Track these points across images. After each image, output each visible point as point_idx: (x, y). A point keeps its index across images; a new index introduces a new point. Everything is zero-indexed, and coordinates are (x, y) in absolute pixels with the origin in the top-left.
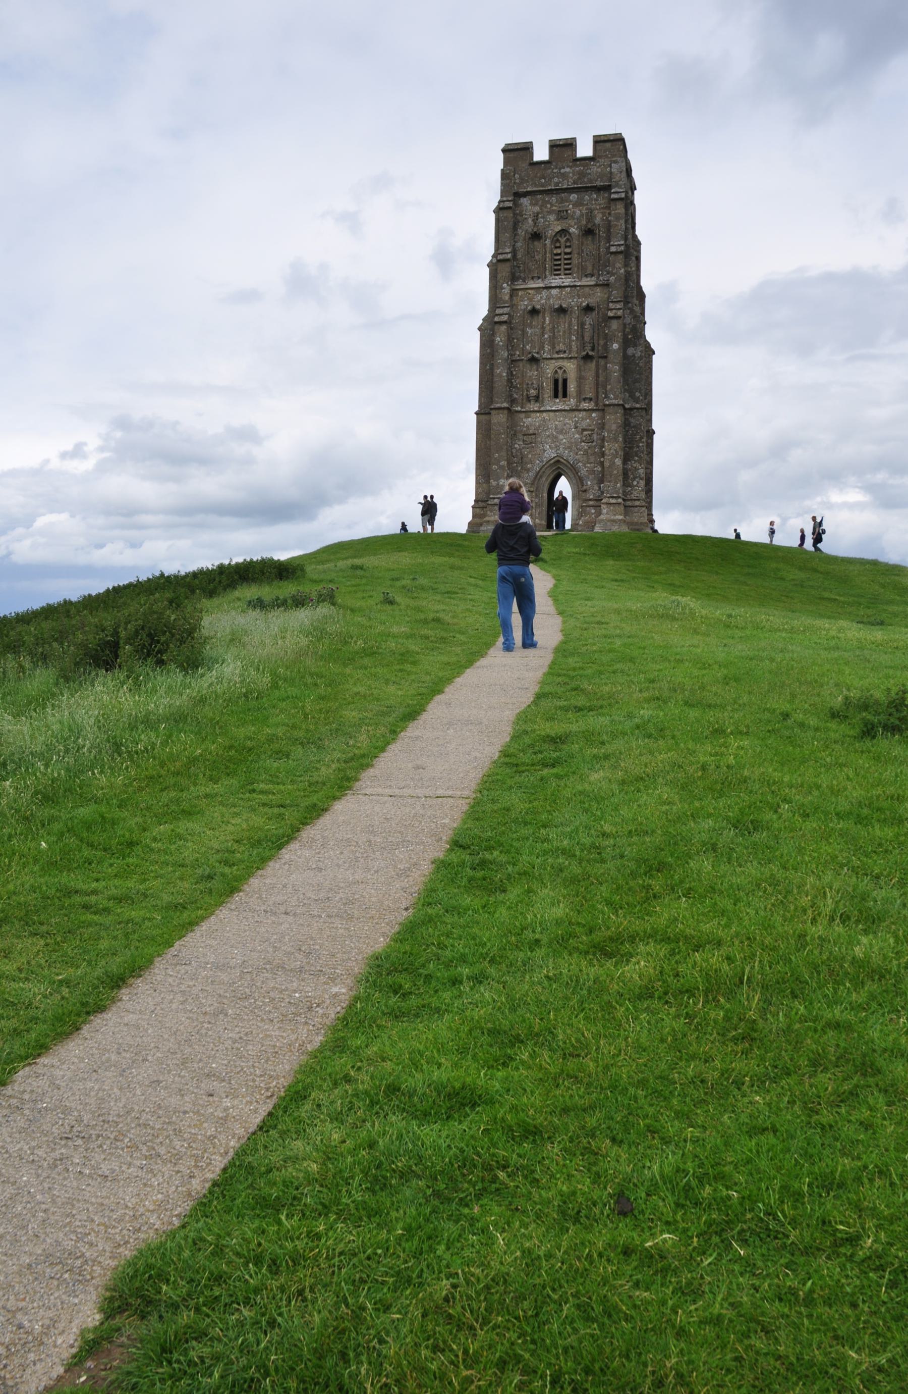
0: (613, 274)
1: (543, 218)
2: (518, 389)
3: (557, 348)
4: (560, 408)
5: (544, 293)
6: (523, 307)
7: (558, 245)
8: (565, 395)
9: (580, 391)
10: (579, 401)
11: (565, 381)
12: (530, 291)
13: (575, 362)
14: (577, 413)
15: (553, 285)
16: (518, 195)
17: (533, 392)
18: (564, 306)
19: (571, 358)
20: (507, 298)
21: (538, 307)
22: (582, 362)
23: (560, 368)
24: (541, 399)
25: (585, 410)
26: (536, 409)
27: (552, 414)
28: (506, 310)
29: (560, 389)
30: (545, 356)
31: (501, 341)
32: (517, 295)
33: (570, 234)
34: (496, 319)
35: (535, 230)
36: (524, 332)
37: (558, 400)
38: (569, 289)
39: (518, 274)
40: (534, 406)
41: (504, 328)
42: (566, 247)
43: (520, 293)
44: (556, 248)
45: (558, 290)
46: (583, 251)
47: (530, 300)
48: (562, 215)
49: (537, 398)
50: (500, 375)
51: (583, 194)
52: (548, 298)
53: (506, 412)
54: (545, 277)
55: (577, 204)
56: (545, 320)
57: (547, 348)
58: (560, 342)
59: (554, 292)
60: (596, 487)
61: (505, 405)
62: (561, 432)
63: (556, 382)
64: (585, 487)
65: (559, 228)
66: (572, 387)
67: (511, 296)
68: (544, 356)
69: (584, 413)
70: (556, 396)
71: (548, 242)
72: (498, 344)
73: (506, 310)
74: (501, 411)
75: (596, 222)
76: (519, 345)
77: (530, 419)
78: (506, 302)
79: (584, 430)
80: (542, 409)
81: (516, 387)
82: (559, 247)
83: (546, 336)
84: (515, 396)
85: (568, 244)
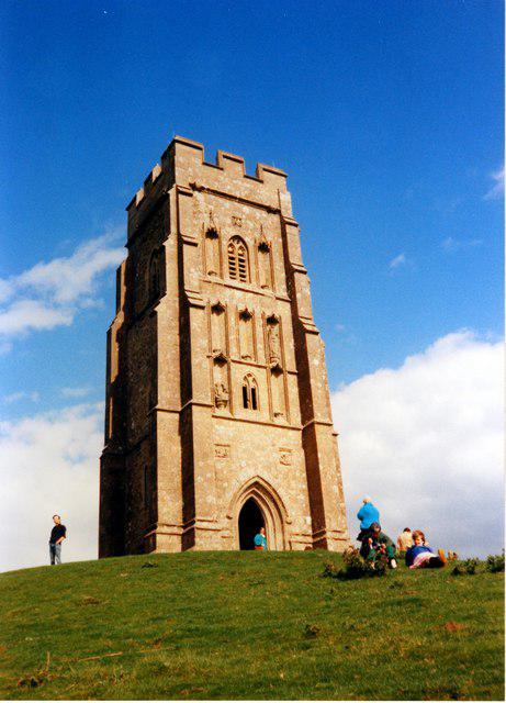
7: (230, 249)
9: (270, 405)
11: (253, 390)
16: (193, 186)
17: (225, 397)
19: (260, 367)
21: (223, 303)
23: (249, 375)
33: (244, 242)
48: (236, 222)
51: (255, 210)
55: (251, 218)
60: (301, 521)
62: (258, 448)
63: (244, 389)
64: (289, 519)
66: (262, 397)
71: (225, 243)
77: (222, 427)
79: (282, 450)
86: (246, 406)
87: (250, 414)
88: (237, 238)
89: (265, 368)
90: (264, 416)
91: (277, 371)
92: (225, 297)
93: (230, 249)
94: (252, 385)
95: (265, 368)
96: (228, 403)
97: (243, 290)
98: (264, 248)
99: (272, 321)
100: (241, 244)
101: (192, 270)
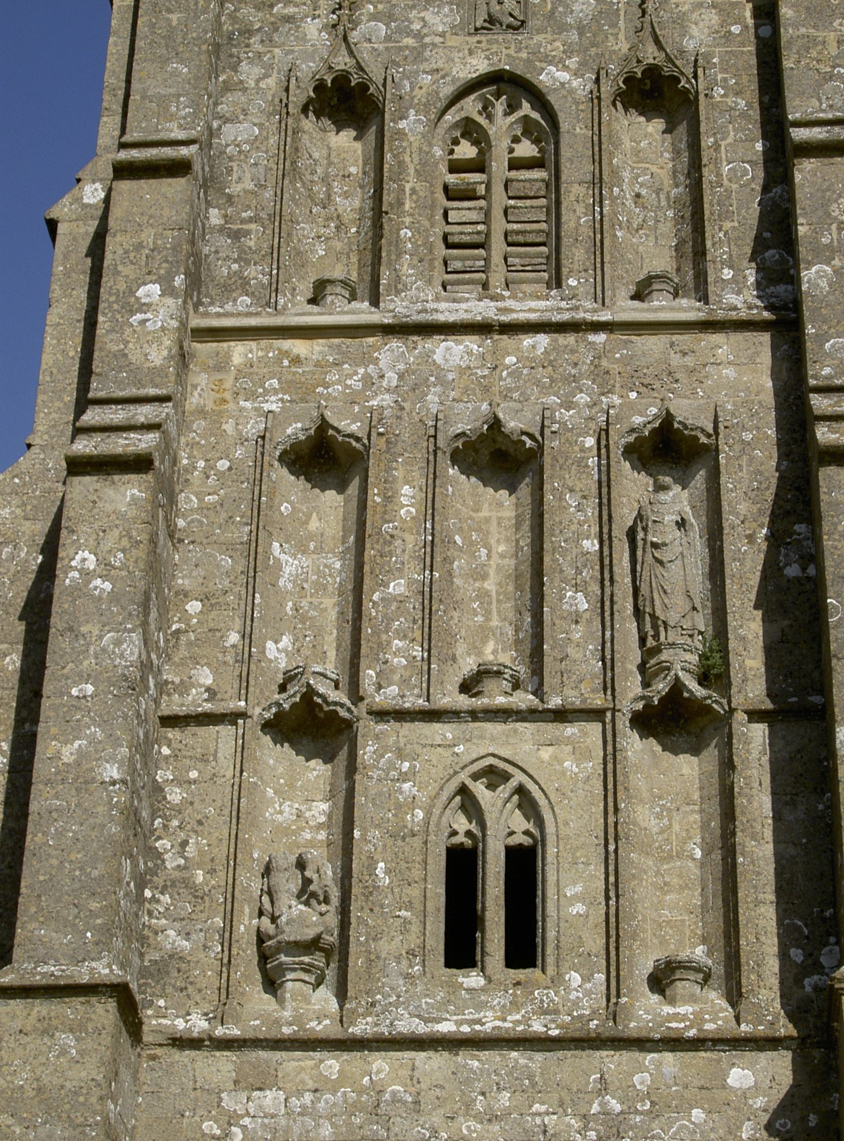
0: (825, 254)
1: (388, 17)
2: (198, 895)
3: (468, 665)
4: (490, 1023)
5: (391, 355)
6: (253, 428)
7: (466, 151)
8: (523, 950)
10: (615, 986)
12: (299, 347)
13: (591, 733)
14: (612, 1061)
15: (441, 318)
17: (301, 919)
18: (512, 424)
19: (561, 715)
20: (158, 355)
21: (349, 425)
22: (636, 747)
24: (357, 962)
25: (674, 1043)
26: (319, 1027)
27: (430, 1063)
28: (143, 413)
29: (491, 906)
30: (388, 696)
31: (106, 568)
32: (221, 365)
34: (84, 446)
35: (342, 62)
36: (255, 566)
37: (473, 979)
38: (543, 340)
39: (223, 270)
40: (311, 1005)
41: (129, 492)
42: (515, 164)
43: (239, 352)
44: (456, 167)
45: (472, 343)
46: (615, 172)
47: (300, 390)
49: (332, 955)
50: (82, 778)
52: (413, 384)
53: (105, 1012)
54: (398, 287)
56: (389, 499)
57: (401, 651)
58: (484, 633)
59: (450, 352)
61: (103, 970)
63: (462, 865)
65: (480, 66)
66: (570, 897)
67: (183, 359)
68: (380, 700)
69: (669, 1062)
70: (461, 951)
72: (79, 591)
73: (143, 413)
74: (70, 1009)
75: (690, 45)
76: (216, 633)
77: (270, 1098)
78: (157, 373)
80: (361, 1028)
81: (181, 883)
82: (479, 166)
83: (397, 587)
84: (172, 939)
85: (526, 149)
86: (461, 951)
87: (486, 998)
88: (508, 84)
89: (596, 714)
90: (573, 990)
91: (673, 720)
92: (361, 389)
93: (466, 151)
94: (505, 825)
95: (596, 714)
96: (332, 955)
97: (482, 328)
98: (657, 92)
99: (669, 449)
100: (526, 108)
101: (151, 291)
